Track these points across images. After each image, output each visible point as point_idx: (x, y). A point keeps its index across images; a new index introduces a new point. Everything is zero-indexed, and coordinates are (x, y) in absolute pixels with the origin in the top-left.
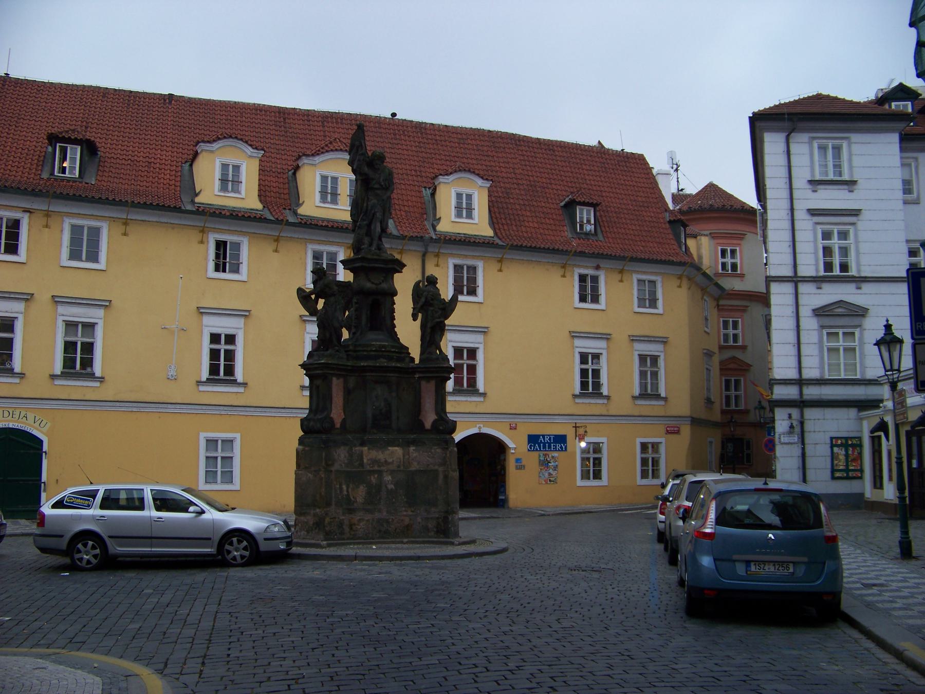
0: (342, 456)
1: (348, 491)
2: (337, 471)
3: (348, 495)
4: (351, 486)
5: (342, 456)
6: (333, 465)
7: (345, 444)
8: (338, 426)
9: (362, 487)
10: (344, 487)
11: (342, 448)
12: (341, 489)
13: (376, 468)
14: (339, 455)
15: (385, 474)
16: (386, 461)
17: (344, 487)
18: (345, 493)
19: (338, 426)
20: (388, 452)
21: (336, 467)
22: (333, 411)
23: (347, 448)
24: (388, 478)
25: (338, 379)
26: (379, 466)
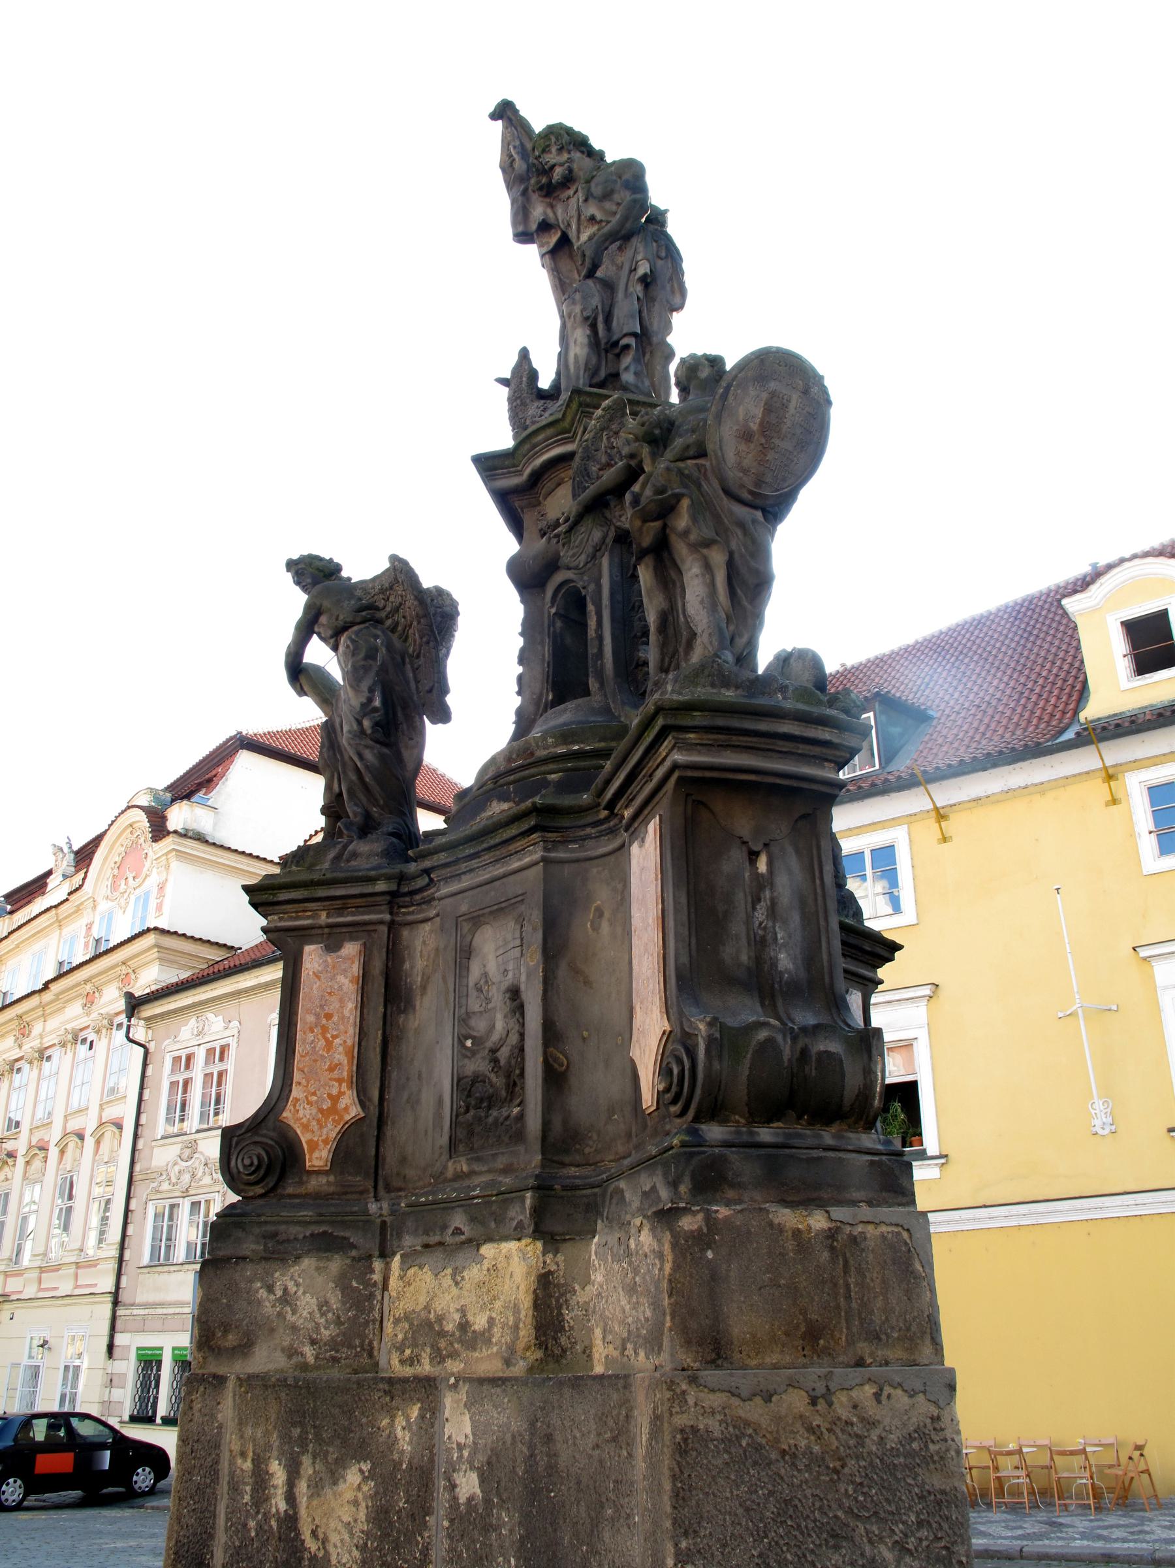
0: (307, 1303)
1: (291, 1498)
2: (248, 1381)
3: (291, 1521)
4: (308, 1467)
5: (307, 1303)
6: (245, 1348)
7: (325, 1244)
8: (318, 1157)
9: (353, 1476)
10: (278, 1472)
11: (307, 1263)
12: (261, 1479)
13: (426, 1367)
14: (286, 1299)
15: (448, 1400)
16: (464, 1326)
17: (278, 1472)
18: (279, 1504)
19: (318, 1157)
20: (474, 1273)
21: (266, 1359)
22: (296, 1092)
23: (336, 1264)
24: (458, 1425)
25: (333, 946)
26: (439, 1357)
